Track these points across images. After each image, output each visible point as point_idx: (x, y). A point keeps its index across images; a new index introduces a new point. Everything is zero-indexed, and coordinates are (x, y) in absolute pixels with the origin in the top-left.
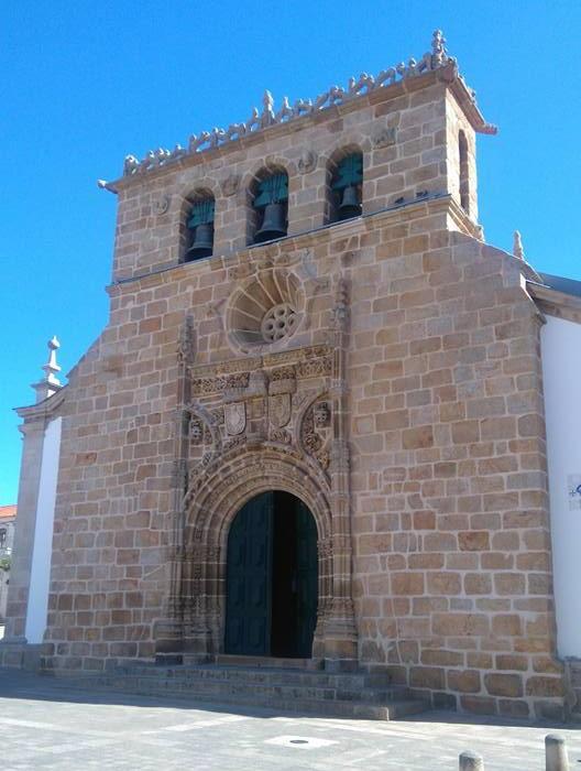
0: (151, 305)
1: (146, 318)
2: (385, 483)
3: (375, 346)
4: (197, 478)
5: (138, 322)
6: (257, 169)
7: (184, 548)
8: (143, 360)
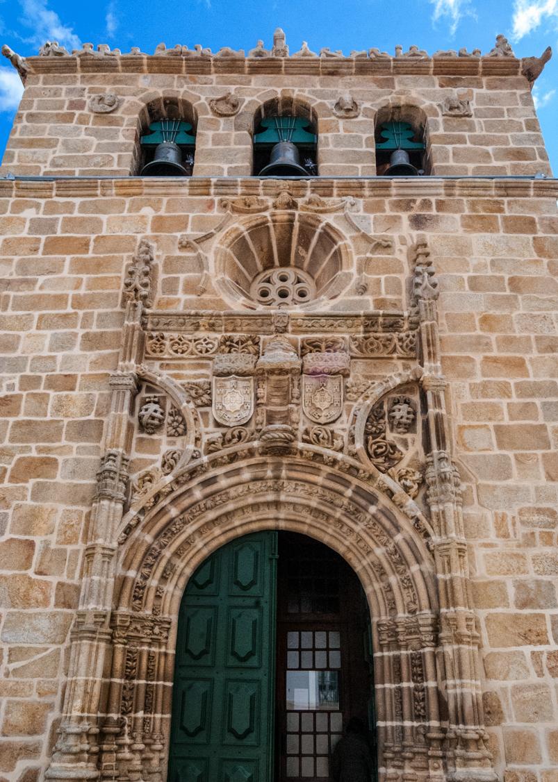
0: (70, 220)
1: (59, 234)
2: (522, 530)
3: (479, 332)
4: (153, 488)
5: (43, 237)
6: (268, 99)
7: (113, 617)
8: (46, 292)
